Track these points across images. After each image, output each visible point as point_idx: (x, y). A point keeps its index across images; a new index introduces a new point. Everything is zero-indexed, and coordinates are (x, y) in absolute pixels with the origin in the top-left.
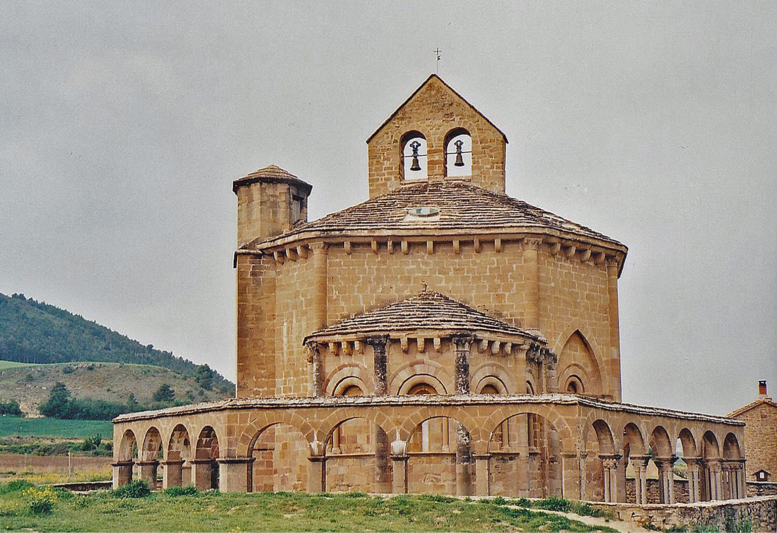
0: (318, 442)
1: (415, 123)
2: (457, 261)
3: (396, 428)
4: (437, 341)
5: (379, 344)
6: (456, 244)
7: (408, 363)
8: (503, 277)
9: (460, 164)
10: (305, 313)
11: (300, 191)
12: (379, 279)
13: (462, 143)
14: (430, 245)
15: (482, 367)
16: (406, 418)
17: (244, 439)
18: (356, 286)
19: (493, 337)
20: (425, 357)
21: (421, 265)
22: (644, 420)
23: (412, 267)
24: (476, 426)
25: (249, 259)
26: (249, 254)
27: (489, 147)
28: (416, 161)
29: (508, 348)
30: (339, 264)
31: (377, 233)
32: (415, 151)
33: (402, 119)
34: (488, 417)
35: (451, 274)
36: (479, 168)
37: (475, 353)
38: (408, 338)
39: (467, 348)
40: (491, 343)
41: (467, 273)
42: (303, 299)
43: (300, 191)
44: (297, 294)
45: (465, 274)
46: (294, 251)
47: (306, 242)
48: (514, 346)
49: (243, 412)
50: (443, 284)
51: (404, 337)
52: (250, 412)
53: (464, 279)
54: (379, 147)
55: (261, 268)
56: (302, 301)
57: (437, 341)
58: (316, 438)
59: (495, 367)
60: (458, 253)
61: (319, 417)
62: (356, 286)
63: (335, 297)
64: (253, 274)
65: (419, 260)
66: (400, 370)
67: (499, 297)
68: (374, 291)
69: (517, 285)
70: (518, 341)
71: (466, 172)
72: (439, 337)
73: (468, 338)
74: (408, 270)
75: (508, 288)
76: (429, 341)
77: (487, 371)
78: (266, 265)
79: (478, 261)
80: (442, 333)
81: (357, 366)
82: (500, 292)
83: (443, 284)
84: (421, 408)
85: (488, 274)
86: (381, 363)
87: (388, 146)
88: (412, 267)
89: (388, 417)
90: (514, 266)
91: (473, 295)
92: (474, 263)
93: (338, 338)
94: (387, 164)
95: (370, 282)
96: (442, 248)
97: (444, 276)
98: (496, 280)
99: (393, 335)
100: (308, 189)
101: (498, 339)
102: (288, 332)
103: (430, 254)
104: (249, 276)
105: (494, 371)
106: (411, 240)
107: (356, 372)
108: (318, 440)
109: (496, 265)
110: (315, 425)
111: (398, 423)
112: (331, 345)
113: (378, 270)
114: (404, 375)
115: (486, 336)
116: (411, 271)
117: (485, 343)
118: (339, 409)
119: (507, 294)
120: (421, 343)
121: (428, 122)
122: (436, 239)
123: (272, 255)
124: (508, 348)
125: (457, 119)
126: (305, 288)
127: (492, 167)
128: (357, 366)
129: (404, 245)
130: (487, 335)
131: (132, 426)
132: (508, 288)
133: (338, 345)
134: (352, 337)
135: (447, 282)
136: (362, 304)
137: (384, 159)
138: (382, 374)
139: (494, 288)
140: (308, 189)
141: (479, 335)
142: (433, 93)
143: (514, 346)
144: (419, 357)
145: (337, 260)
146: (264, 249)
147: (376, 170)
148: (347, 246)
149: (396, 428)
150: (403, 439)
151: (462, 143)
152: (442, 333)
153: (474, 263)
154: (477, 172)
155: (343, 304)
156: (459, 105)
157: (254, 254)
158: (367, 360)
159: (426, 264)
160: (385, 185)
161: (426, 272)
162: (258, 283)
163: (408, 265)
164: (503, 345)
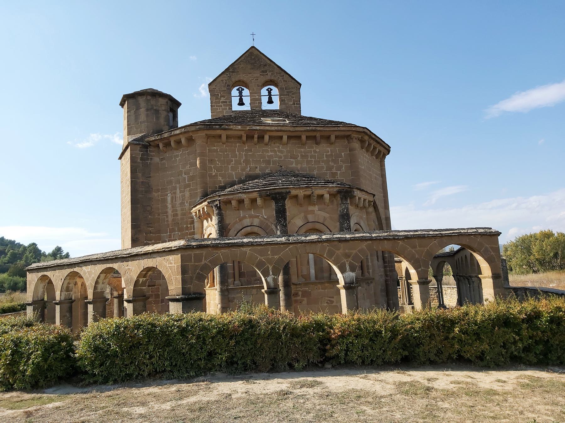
0: (273, 276)
2: (302, 150)
4: (327, 196)
10: (189, 186)
11: (174, 105)
13: (271, 90)
14: (285, 138)
16: (354, 252)
18: (230, 166)
20: (316, 208)
24: (417, 256)
26: (140, 144)
30: (216, 151)
32: (241, 93)
33: (233, 72)
36: (285, 104)
42: (186, 176)
43: (174, 105)
44: (180, 174)
45: (309, 159)
47: (191, 134)
49: (198, 252)
52: (204, 252)
53: (308, 162)
55: (148, 155)
56: (185, 178)
58: (271, 273)
60: (304, 145)
62: (230, 166)
63: (214, 174)
64: (141, 159)
75: (339, 168)
78: (152, 154)
79: (318, 150)
81: (258, 217)
82: (334, 171)
83: (294, 165)
84: (366, 243)
85: (325, 159)
86: (281, 214)
90: (343, 154)
96: (292, 141)
98: (330, 163)
99: (294, 192)
100: (178, 104)
102: (172, 201)
104: (139, 161)
111: (347, 256)
112: (234, 203)
118: (291, 246)
119: (339, 172)
122: (290, 134)
123: (158, 146)
125: (270, 74)
126: (188, 167)
129: (267, 138)
132: (339, 168)
133: (241, 202)
134: (255, 195)
135: (296, 164)
136: (235, 179)
139: (330, 168)
140: (178, 104)
144: (311, 208)
145: (215, 148)
146: (151, 141)
151: (271, 90)
154: (284, 106)
155: (220, 178)
158: (268, 213)
159: (281, 152)
161: (281, 157)
163: (268, 152)
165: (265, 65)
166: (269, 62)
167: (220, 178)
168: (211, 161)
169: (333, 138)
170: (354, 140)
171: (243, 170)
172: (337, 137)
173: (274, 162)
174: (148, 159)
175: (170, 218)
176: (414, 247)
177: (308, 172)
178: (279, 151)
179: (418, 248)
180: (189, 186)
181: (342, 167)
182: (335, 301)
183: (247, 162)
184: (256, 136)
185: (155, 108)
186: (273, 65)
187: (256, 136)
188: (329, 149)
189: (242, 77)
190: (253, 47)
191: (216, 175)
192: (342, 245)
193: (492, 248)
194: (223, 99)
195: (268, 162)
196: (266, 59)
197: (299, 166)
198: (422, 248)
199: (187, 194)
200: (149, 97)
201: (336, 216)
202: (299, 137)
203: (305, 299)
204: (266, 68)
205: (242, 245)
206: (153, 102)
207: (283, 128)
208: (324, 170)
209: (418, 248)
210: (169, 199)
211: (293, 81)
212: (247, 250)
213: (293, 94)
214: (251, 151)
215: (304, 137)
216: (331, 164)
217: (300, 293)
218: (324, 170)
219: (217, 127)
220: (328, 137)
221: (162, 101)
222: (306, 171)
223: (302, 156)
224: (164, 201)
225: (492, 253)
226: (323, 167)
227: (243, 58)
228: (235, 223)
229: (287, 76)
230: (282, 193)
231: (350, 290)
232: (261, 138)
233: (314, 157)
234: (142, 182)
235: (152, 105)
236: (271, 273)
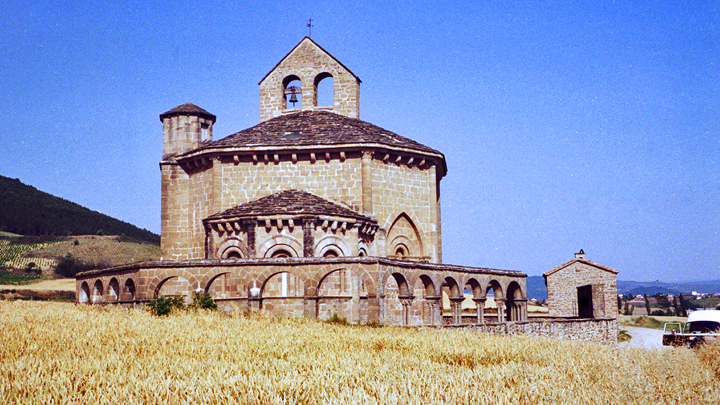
4: (291, 222)
5: (247, 226)
17: (151, 287)
19: (332, 218)
22: (435, 272)
23: (281, 171)
25: (169, 166)
29: (344, 226)
31: (256, 149)
33: (284, 67)
40: (331, 223)
46: (200, 161)
50: (304, 182)
52: (155, 270)
53: (319, 179)
57: (291, 222)
64: (173, 177)
67: (345, 191)
68: (255, 187)
77: (329, 241)
81: (236, 239)
82: (345, 187)
83: (304, 182)
86: (252, 239)
92: (326, 168)
93: (223, 220)
94: (273, 99)
99: (260, 218)
105: (333, 241)
107: (237, 243)
110: (199, 278)
111: (255, 276)
114: (268, 245)
116: (282, 174)
117: (326, 223)
120: (280, 223)
124: (344, 226)
125: (323, 66)
128: (236, 239)
130: (327, 217)
131: (88, 281)
132: (350, 184)
135: (307, 180)
137: (272, 95)
139: (340, 184)
141: (321, 217)
147: (265, 103)
150: (258, 286)
155: (233, 197)
160: (271, 113)
164: (340, 224)
165: (319, 57)
167: (233, 197)
169: (342, 154)
171: (255, 187)
175: (195, 233)
176: (306, 270)
178: (291, 168)
180: (207, 204)
183: (259, 179)
191: (229, 194)
192: (252, 267)
195: (279, 179)
197: (309, 183)
199: (206, 210)
204: (320, 60)
210: (194, 215)
214: (263, 168)
216: (342, 180)
218: (334, 187)
221: (193, 118)
224: (190, 216)
226: (333, 184)
228: (222, 243)
230: (250, 219)
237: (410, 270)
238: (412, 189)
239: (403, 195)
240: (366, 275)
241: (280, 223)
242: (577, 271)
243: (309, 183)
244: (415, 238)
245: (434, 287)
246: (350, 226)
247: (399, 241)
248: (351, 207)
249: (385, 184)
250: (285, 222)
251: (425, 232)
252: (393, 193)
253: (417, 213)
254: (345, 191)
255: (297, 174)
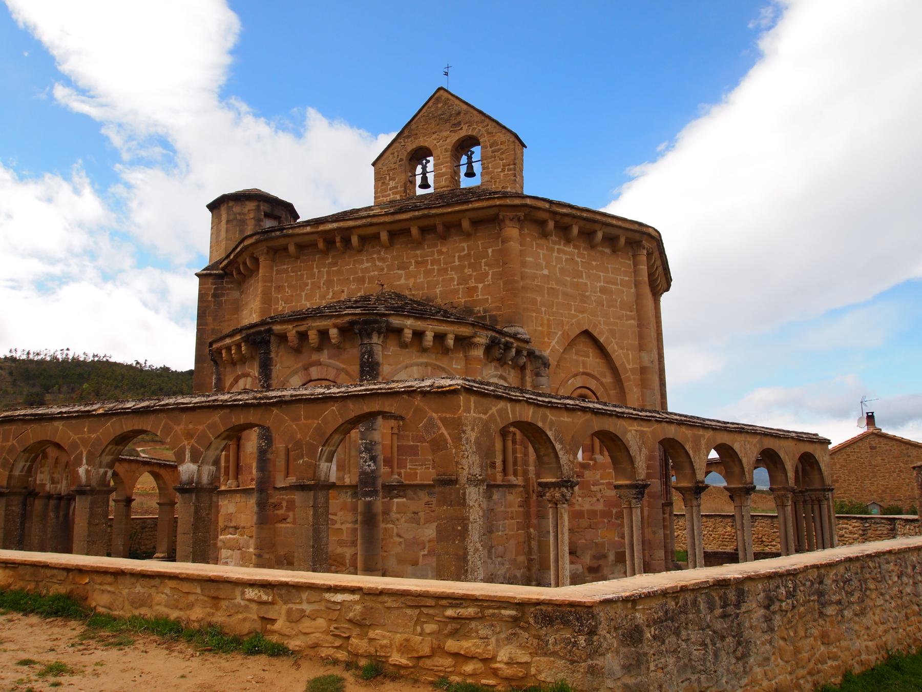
0: (86, 467)
1: (421, 139)
2: (418, 252)
3: (186, 443)
4: (333, 332)
6: (415, 231)
7: (300, 365)
8: (474, 266)
9: (470, 174)
12: (329, 283)
14: (384, 236)
15: (406, 367)
16: (201, 428)
19: (420, 325)
20: (324, 357)
21: (377, 263)
23: (366, 265)
24: (299, 436)
27: (499, 150)
28: (425, 179)
29: (450, 342)
33: (408, 137)
34: (316, 422)
35: (412, 268)
36: (488, 173)
37: (393, 348)
38: (297, 332)
39: (375, 339)
41: (432, 265)
45: (429, 267)
48: (459, 339)
50: (403, 281)
51: (291, 331)
53: (428, 273)
54: (385, 168)
57: (333, 332)
58: (84, 461)
59: (429, 368)
60: (418, 244)
61: (91, 431)
62: (303, 294)
64: (214, 296)
65: (375, 256)
66: (291, 375)
67: (471, 291)
69: (493, 274)
70: (465, 331)
71: (475, 182)
72: (335, 326)
73: (376, 326)
74: (362, 269)
75: (481, 278)
76: (324, 334)
79: (444, 250)
80: (339, 321)
82: (472, 284)
83: (403, 281)
84: (221, 412)
85: (457, 263)
87: (393, 166)
88: (366, 265)
89: (176, 428)
90: (490, 251)
91: (438, 291)
94: (392, 184)
95: (319, 287)
97: (403, 272)
98: (466, 271)
101: (430, 329)
103: (387, 248)
104: (210, 298)
106: (363, 232)
108: (88, 463)
109: (466, 252)
111: (189, 435)
113: (328, 273)
115: (409, 324)
117: (408, 334)
119: (480, 286)
120: (313, 336)
121: (434, 136)
124: (450, 342)
127: (503, 170)
129: (355, 240)
132: (481, 278)
135: (407, 279)
137: (390, 180)
138: (265, 381)
139: (464, 280)
141: (396, 321)
142: (440, 105)
143: (459, 339)
144: (315, 357)
145: (285, 267)
148: (292, 248)
149: (186, 443)
150: (194, 460)
152: (339, 321)
153: (440, 253)
156: (466, 113)
157: (215, 274)
159: (383, 260)
161: (382, 269)
162: (219, 305)
163: (362, 263)
164: (440, 337)
165: (459, 113)
166: (464, 107)
168: (279, 288)
169: (466, 224)
170: (508, 222)
171: (323, 297)
172: (476, 223)
173: (371, 279)
174: (223, 295)
176: (296, 419)
177: (426, 291)
179: (303, 421)
181: (487, 274)
182: (338, 521)
183: (329, 283)
184: (338, 239)
185: (238, 217)
186: (471, 110)
187: (338, 239)
188: (465, 245)
189: (423, 141)
190: (440, 89)
192: (184, 417)
193: (443, 420)
194: (392, 184)
196: (461, 104)
198: (310, 421)
200: (231, 204)
201: (355, 369)
202: (407, 231)
203: (291, 514)
204: (459, 118)
205: (51, 418)
206: (237, 209)
207: (375, 220)
208: (454, 285)
209: (303, 421)
211: (504, 131)
212: (59, 425)
213: (502, 153)
214: (335, 264)
215: (415, 231)
216: (468, 271)
217: (284, 504)
218: (454, 285)
219: (278, 233)
220: (459, 225)
221: (251, 205)
222: (423, 289)
223: (417, 263)
225: (443, 430)
226: (452, 279)
227: (424, 110)
229: (494, 124)
230: (260, 332)
231: (187, 495)
232: (347, 241)
233: (437, 262)
234: (213, 330)
235: (235, 214)
236: (84, 461)
237: (566, 418)
238: (603, 290)
239: (584, 299)
240: (431, 422)
241: (313, 336)
242: (872, 448)
243: (411, 282)
244: (608, 379)
245: (631, 460)
246: (463, 342)
247: (579, 382)
248: (484, 318)
249: (548, 278)
250: (324, 334)
251: (629, 366)
252: (565, 294)
253: (612, 332)
254: (471, 291)
255: (390, 268)
